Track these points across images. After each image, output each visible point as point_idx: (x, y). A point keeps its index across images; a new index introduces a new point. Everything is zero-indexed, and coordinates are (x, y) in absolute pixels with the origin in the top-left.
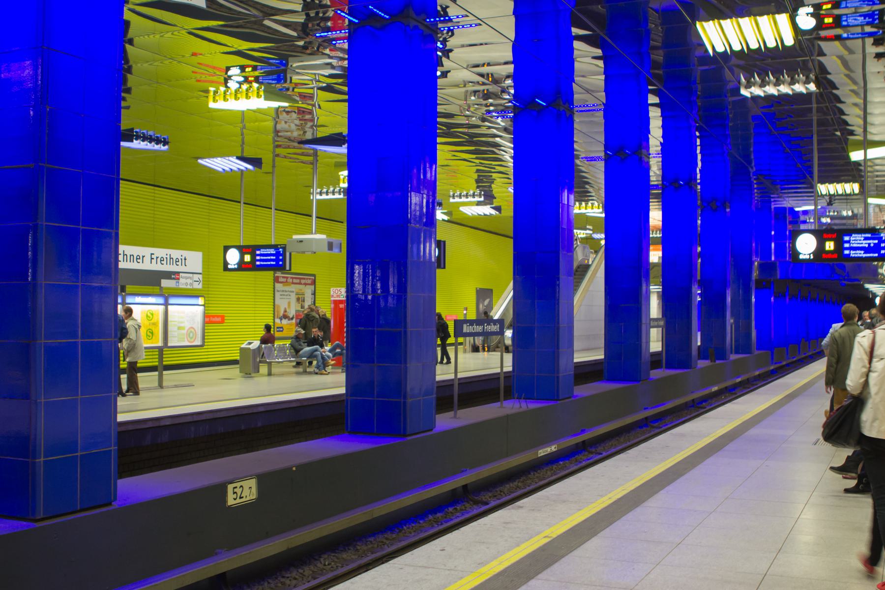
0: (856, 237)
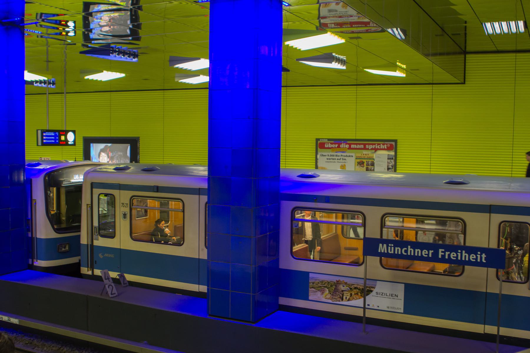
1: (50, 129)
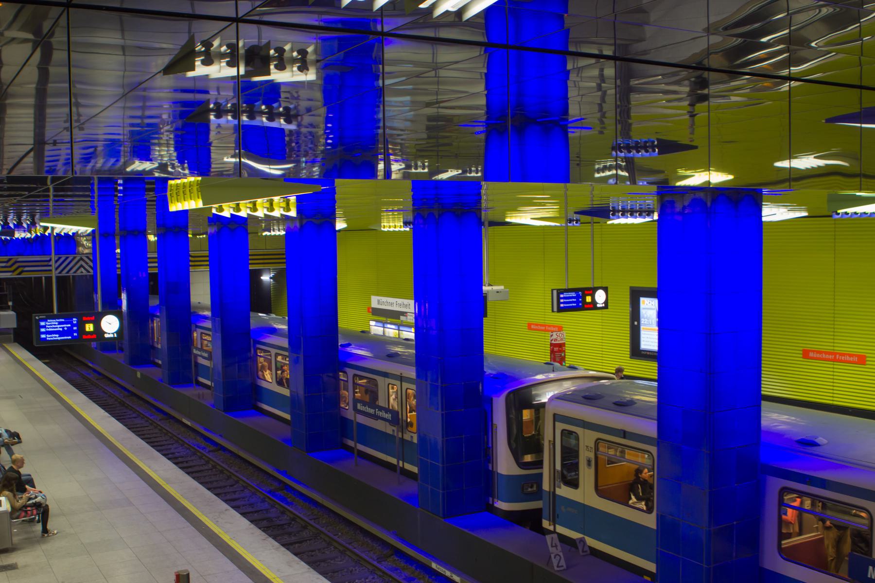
0: (51, 322)
1: (570, 287)
